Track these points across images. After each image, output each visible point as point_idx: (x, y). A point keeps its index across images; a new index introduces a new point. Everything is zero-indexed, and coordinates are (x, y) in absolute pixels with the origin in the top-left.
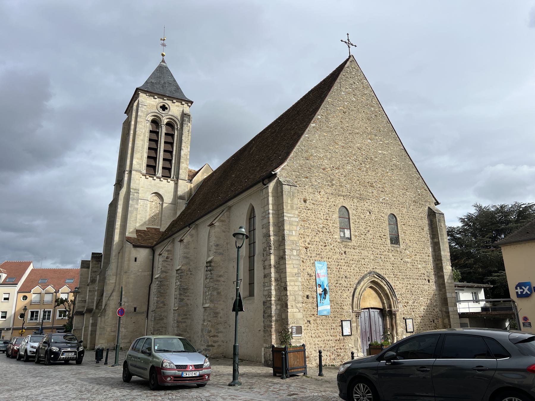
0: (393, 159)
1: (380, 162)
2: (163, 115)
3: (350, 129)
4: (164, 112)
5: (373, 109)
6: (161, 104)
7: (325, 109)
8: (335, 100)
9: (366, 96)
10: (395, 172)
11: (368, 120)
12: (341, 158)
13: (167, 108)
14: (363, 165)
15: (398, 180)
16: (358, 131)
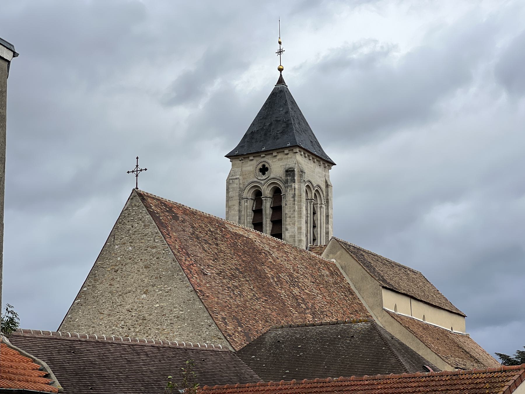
0: (175, 309)
1: (155, 320)
2: (263, 182)
3: (120, 289)
4: (264, 177)
5: (154, 250)
6: (260, 166)
7: (93, 276)
8: (106, 260)
9: (147, 236)
10: (175, 327)
11: (145, 269)
12: (106, 329)
13: (267, 169)
14: (132, 330)
15: (179, 336)
16: (130, 289)
